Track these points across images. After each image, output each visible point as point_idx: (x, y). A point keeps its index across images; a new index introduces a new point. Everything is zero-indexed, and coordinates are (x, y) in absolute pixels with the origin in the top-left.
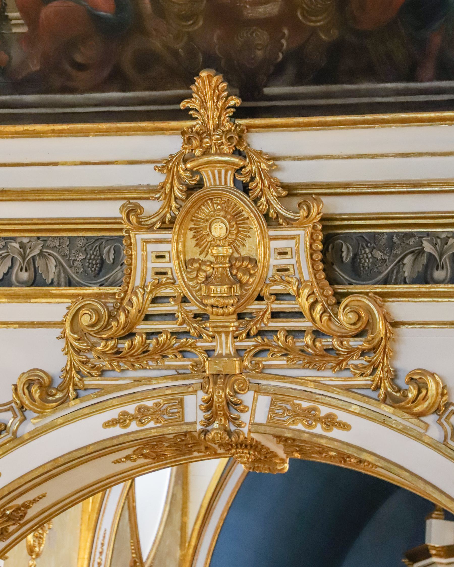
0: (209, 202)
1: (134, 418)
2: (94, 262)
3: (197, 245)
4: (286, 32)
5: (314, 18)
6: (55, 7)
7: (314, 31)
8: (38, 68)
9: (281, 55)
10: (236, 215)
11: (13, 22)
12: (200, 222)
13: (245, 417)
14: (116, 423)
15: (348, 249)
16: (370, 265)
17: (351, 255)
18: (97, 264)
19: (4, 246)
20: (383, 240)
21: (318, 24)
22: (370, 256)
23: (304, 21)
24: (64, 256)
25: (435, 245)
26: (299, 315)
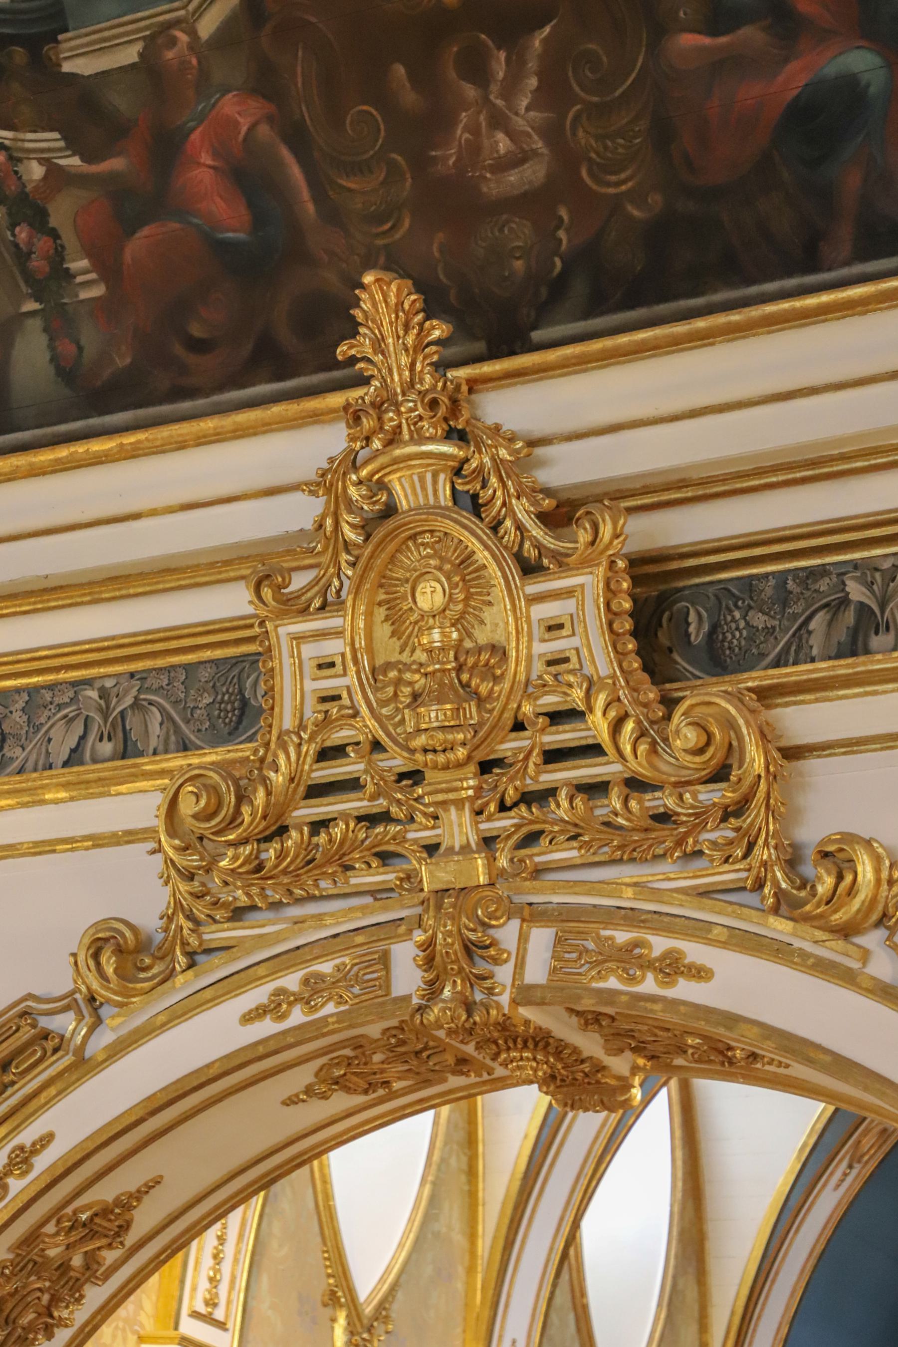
1: (298, 999)
2: (229, 707)
3: (393, 634)
4: (563, 213)
5: (613, 178)
6: (146, 237)
8: (128, 360)
9: (558, 262)
10: (462, 562)
11: (79, 279)
12: (396, 586)
13: (504, 974)
14: (265, 1011)
16: (743, 643)
17: (706, 627)
18: (235, 710)
19: (72, 699)
20: (768, 589)
21: (623, 188)
22: (742, 624)
23: (594, 187)
24: (176, 703)
25: (870, 585)
26: (594, 750)
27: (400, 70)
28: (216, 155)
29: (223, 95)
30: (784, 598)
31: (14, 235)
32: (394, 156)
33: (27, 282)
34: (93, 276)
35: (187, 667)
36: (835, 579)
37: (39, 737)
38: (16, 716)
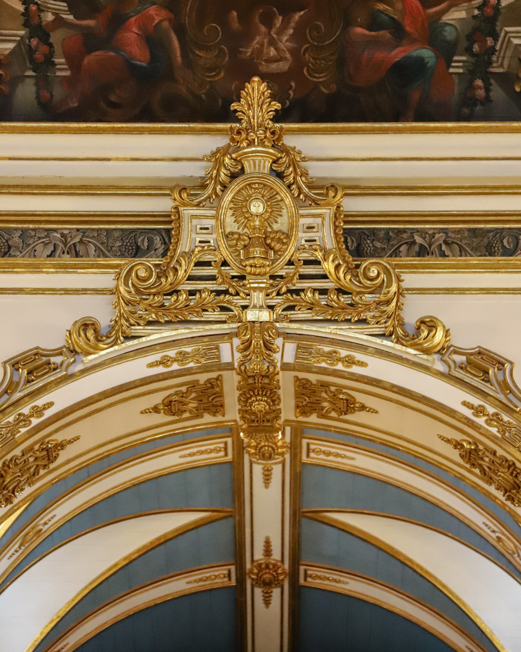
0: (248, 187)
1: (175, 360)
2: (130, 248)
3: (235, 221)
4: (293, 84)
5: (317, 75)
7: (316, 85)
8: (76, 105)
10: (271, 198)
11: (58, 67)
13: (277, 356)
14: (160, 363)
15: (352, 240)
16: (372, 252)
19: (46, 236)
20: (382, 234)
21: (321, 80)
22: (371, 245)
23: (308, 77)
24: (102, 244)
25: (424, 238)
27: (235, 14)
28: (140, 28)
29: (151, 6)
30: (388, 239)
31: (30, 42)
32: (223, 46)
33: (31, 63)
34: (66, 67)
35: (107, 230)
36: (409, 234)
37: (29, 248)
38: (16, 239)
